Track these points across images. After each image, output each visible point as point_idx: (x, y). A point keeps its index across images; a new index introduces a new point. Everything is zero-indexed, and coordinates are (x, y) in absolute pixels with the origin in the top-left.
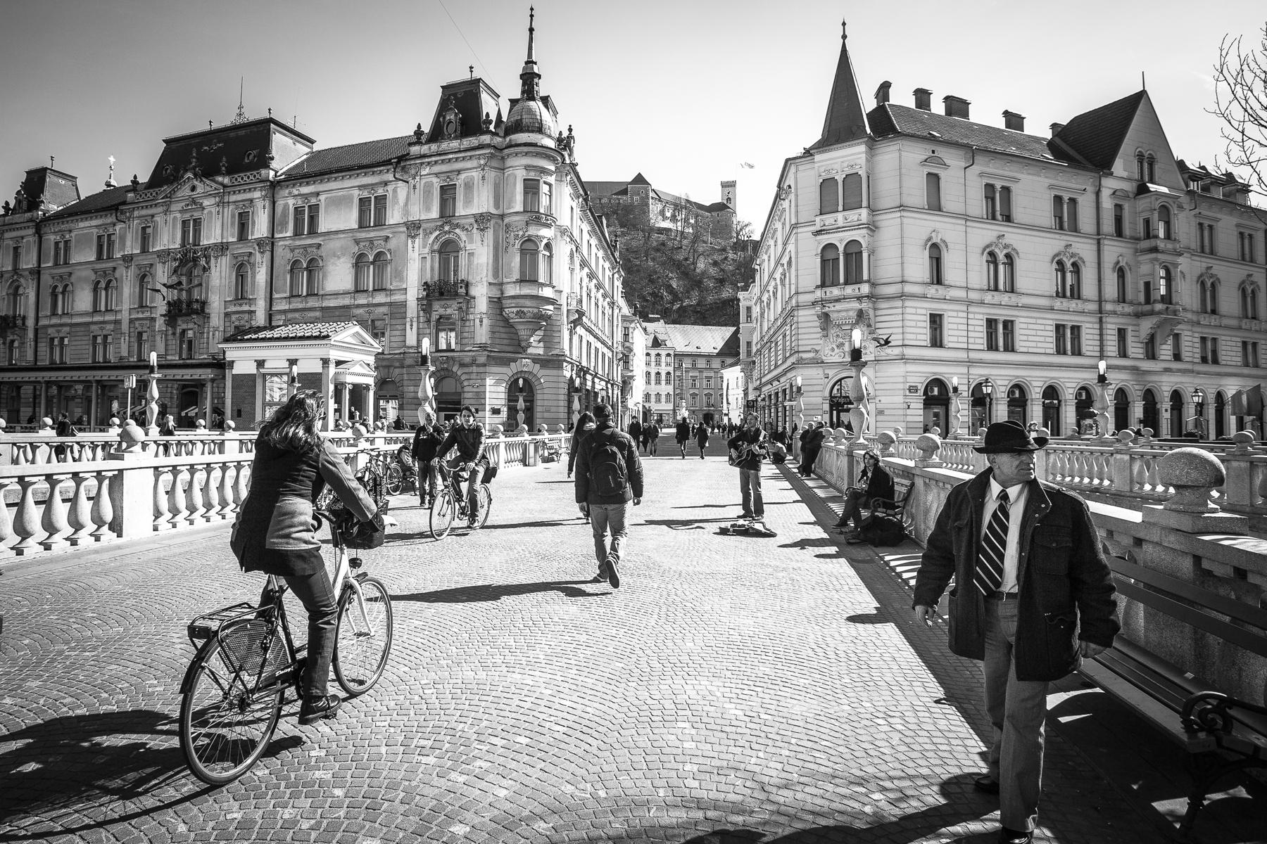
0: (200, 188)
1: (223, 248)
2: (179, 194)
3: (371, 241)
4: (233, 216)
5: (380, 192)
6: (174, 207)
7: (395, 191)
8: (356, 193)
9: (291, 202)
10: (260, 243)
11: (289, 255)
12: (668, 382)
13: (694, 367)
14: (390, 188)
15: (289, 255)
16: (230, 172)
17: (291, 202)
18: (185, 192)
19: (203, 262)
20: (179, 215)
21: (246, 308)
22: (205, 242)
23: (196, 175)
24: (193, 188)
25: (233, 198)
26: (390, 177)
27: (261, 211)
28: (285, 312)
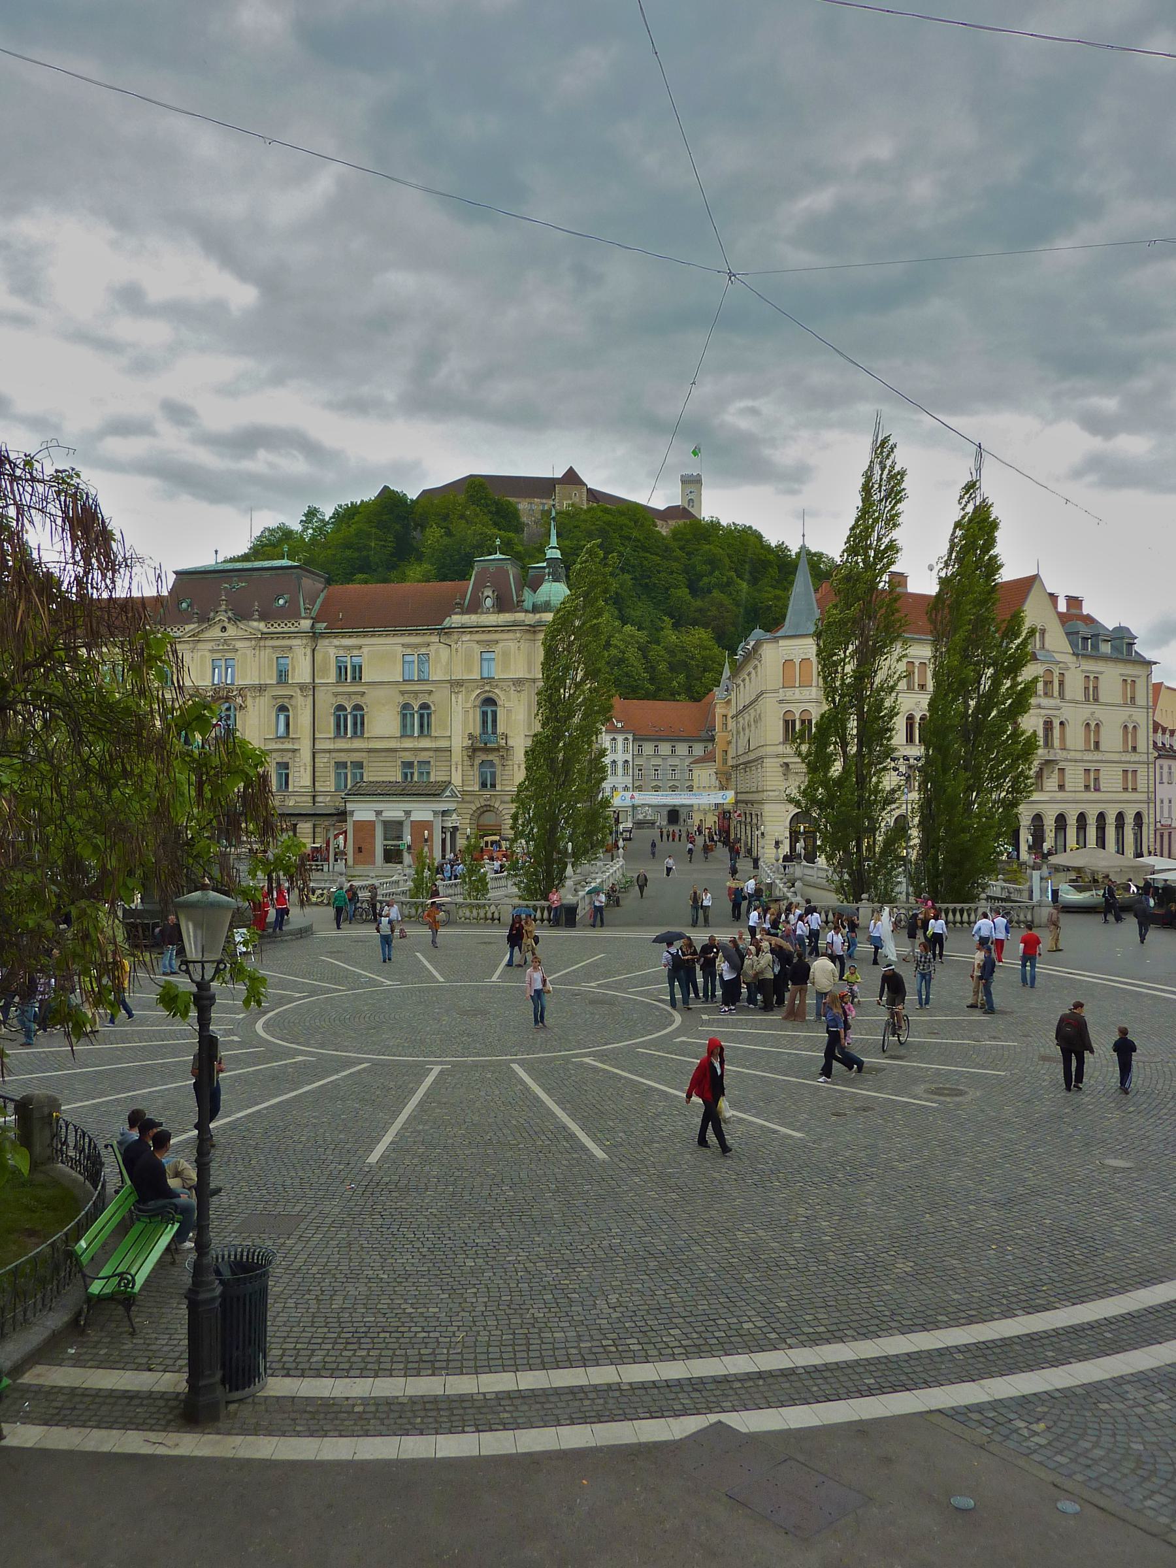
0: (232, 631)
1: (261, 688)
2: (207, 635)
3: (416, 693)
4: (270, 660)
5: (423, 650)
6: (200, 646)
7: (437, 651)
8: (400, 649)
9: (332, 652)
10: (302, 687)
11: (333, 700)
12: (625, 774)
13: (656, 754)
14: (432, 648)
15: (333, 700)
16: (263, 617)
17: (332, 652)
18: (215, 632)
19: (239, 700)
20: (208, 654)
21: (290, 746)
22: (240, 682)
23: (229, 619)
24: (224, 629)
25: (270, 643)
26: (435, 639)
27: (301, 658)
28: (329, 751)
